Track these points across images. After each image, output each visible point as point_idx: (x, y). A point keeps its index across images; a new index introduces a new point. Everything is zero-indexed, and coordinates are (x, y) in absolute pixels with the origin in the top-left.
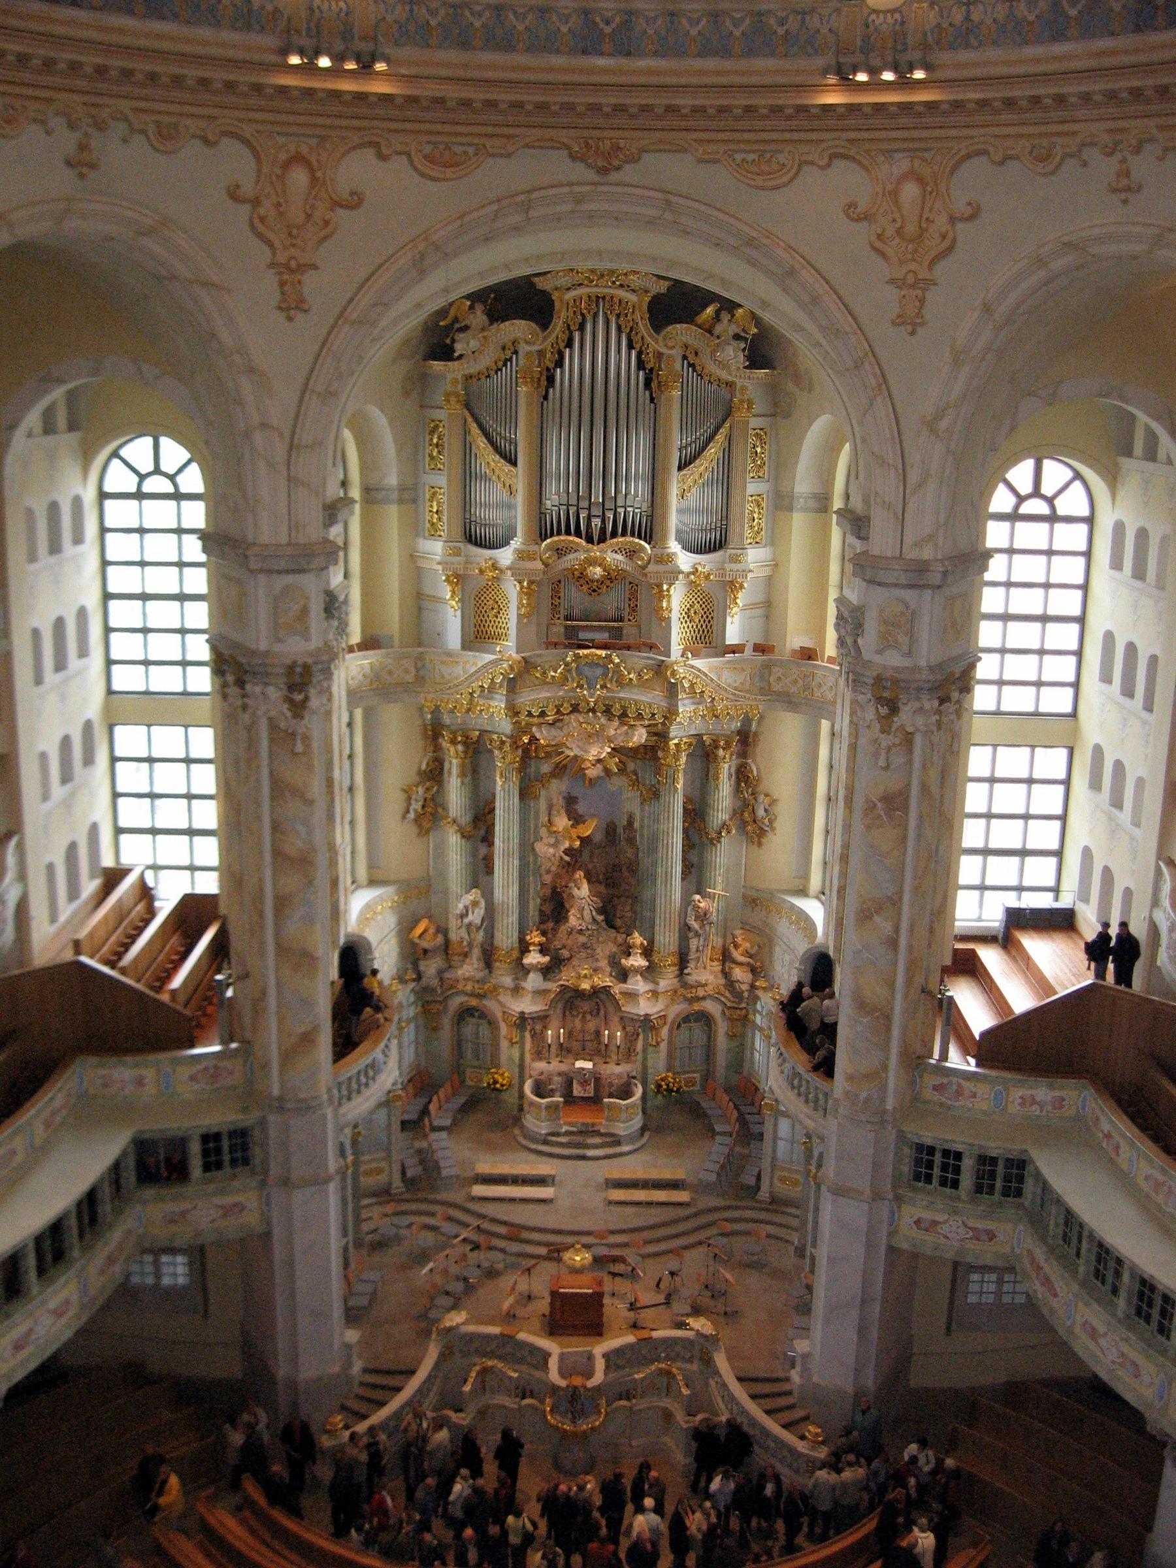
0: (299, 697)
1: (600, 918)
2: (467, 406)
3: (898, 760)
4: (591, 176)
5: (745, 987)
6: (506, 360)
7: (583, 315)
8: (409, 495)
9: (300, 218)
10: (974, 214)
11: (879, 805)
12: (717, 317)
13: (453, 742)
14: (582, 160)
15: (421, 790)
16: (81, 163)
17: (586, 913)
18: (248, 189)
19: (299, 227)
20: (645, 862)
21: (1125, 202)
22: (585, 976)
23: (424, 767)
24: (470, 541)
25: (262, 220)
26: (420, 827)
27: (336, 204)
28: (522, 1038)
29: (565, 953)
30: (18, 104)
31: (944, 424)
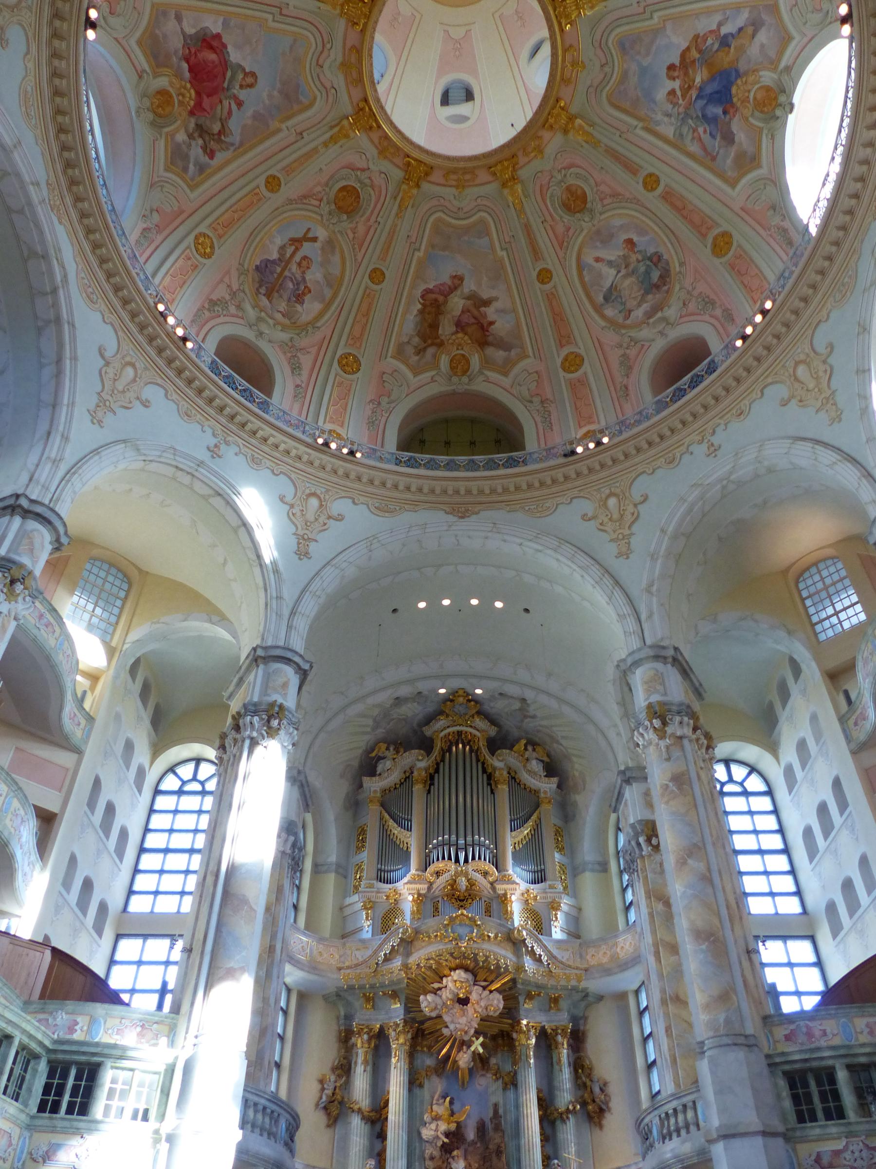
0: (275, 723)
2: (383, 805)
3: (676, 753)
4: (456, 519)
8: (342, 871)
9: (312, 519)
10: (645, 498)
11: (671, 784)
12: (526, 749)
13: (359, 1033)
14: (451, 513)
15: (333, 1078)
16: (214, 451)
18: (289, 498)
19: (311, 523)
21: (716, 456)
25: (293, 514)
26: (329, 1115)
27: (329, 517)
30: (194, 412)
31: (655, 588)
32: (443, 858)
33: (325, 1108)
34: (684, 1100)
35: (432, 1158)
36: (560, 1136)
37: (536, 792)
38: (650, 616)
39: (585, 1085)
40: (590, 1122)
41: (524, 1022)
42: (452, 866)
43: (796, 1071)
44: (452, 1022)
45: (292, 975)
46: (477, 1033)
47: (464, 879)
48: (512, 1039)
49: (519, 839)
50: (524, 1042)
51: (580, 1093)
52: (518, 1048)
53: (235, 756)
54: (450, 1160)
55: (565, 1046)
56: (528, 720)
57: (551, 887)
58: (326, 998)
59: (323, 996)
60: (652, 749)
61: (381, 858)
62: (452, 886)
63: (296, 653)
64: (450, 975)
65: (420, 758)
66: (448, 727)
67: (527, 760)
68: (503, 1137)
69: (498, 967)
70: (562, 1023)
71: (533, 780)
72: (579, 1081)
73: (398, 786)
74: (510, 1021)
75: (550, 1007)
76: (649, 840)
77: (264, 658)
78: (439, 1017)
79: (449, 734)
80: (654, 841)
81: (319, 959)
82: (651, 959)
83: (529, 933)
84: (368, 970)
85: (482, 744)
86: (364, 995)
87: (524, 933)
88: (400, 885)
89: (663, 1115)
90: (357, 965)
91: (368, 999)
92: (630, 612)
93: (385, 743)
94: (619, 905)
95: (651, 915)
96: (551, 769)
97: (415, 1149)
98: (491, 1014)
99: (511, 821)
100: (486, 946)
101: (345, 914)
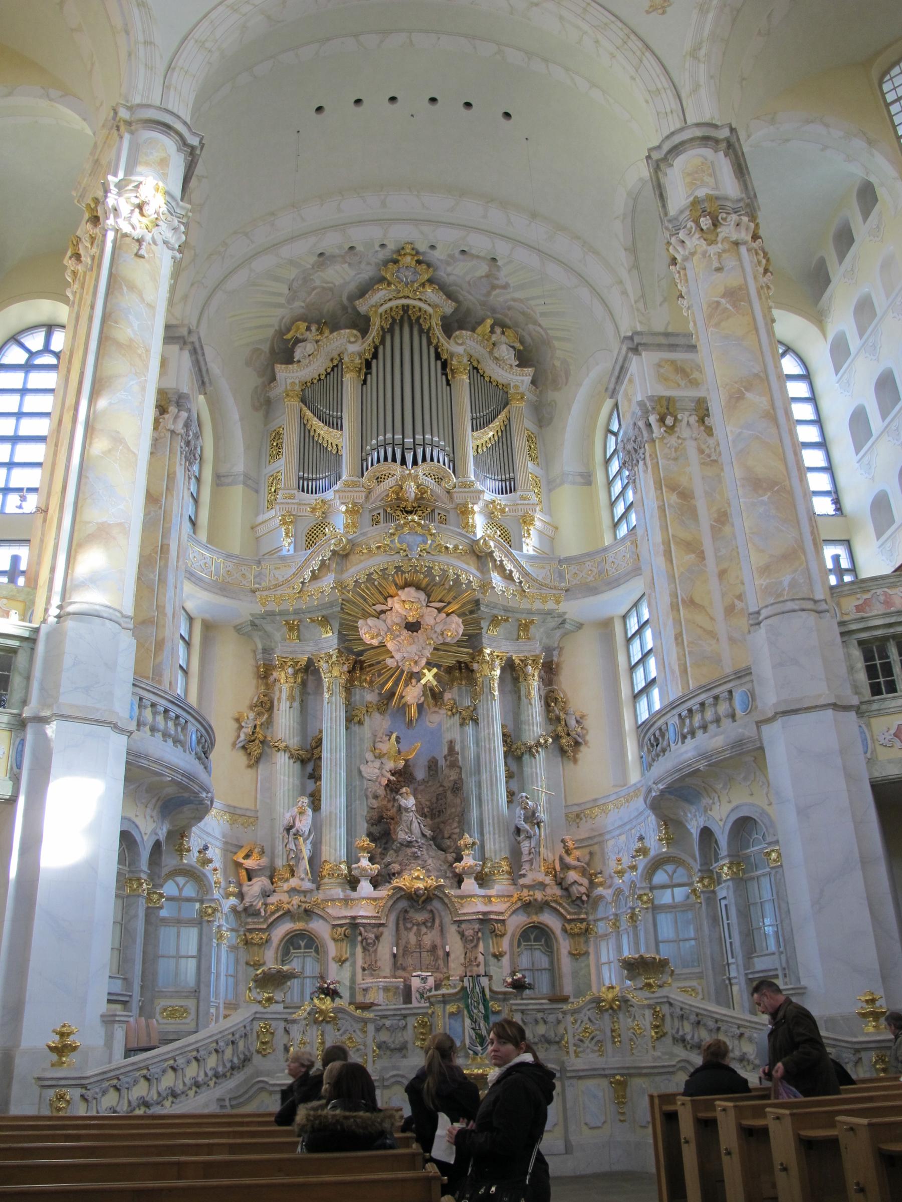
1: (428, 833)
2: (303, 400)
3: (730, 262)
5: (583, 890)
6: (334, 366)
7: (392, 317)
8: (252, 483)
11: (723, 301)
12: (492, 332)
13: (282, 667)
15: (252, 715)
17: (415, 825)
20: (470, 784)
22: (418, 878)
23: (255, 700)
24: (303, 491)
28: (353, 954)
29: (396, 867)
31: (703, 51)
32: (386, 459)
33: (244, 748)
34: (716, 691)
35: (376, 797)
36: (527, 770)
37: (505, 388)
38: (696, 88)
39: (558, 719)
40: (562, 757)
41: (488, 651)
42: (397, 469)
43: (876, 639)
44: (399, 650)
45: (196, 599)
46: (429, 665)
47: (412, 484)
48: (472, 671)
49: (483, 441)
50: (487, 672)
51: (552, 728)
52: (480, 680)
53: (93, 258)
54: (398, 797)
55: (536, 678)
56: (498, 291)
57: (522, 498)
58: (238, 629)
59: (235, 627)
60: (695, 258)
61: (302, 465)
62: (397, 494)
63: (178, 117)
64: (397, 595)
65: (352, 339)
66: (390, 300)
67: (494, 344)
68: (460, 773)
69: (457, 581)
70: (533, 654)
71: (500, 371)
72: (552, 715)
73: (323, 377)
74: (471, 651)
75: (519, 635)
76: (662, 420)
77: (129, 123)
78: (382, 645)
79: (391, 309)
80: (669, 421)
81: (229, 580)
82: (659, 562)
83: (498, 545)
84: (290, 591)
85: (435, 323)
86: (287, 623)
87: (492, 544)
88: (329, 495)
89: (684, 713)
90: (276, 586)
91: (291, 628)
92: (666, 86)
93: (305, 321)
94: (606, 522)
95: (662, 509)
96: (524, 358)
97: (355, 787)
98: (448, 640)
99: (472, 419)
100: (443, 558)
101: (259, 535)
